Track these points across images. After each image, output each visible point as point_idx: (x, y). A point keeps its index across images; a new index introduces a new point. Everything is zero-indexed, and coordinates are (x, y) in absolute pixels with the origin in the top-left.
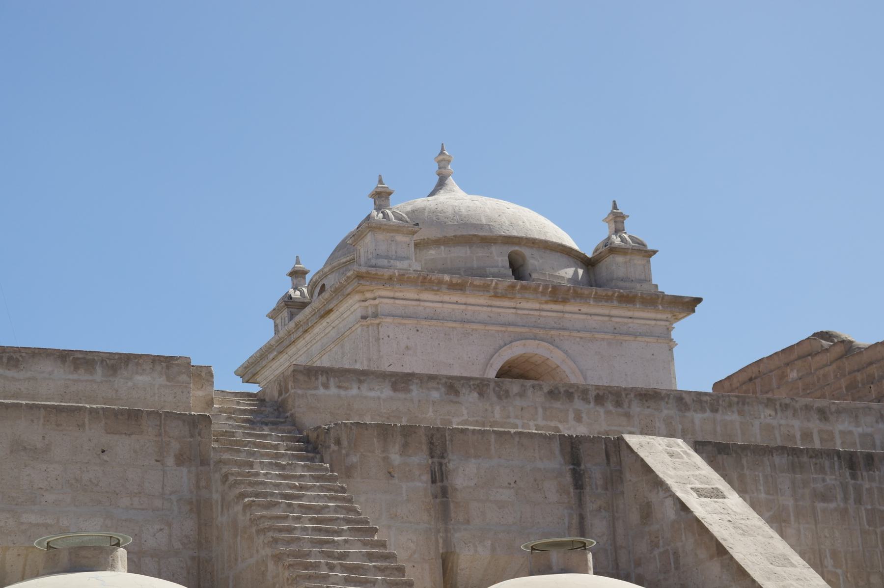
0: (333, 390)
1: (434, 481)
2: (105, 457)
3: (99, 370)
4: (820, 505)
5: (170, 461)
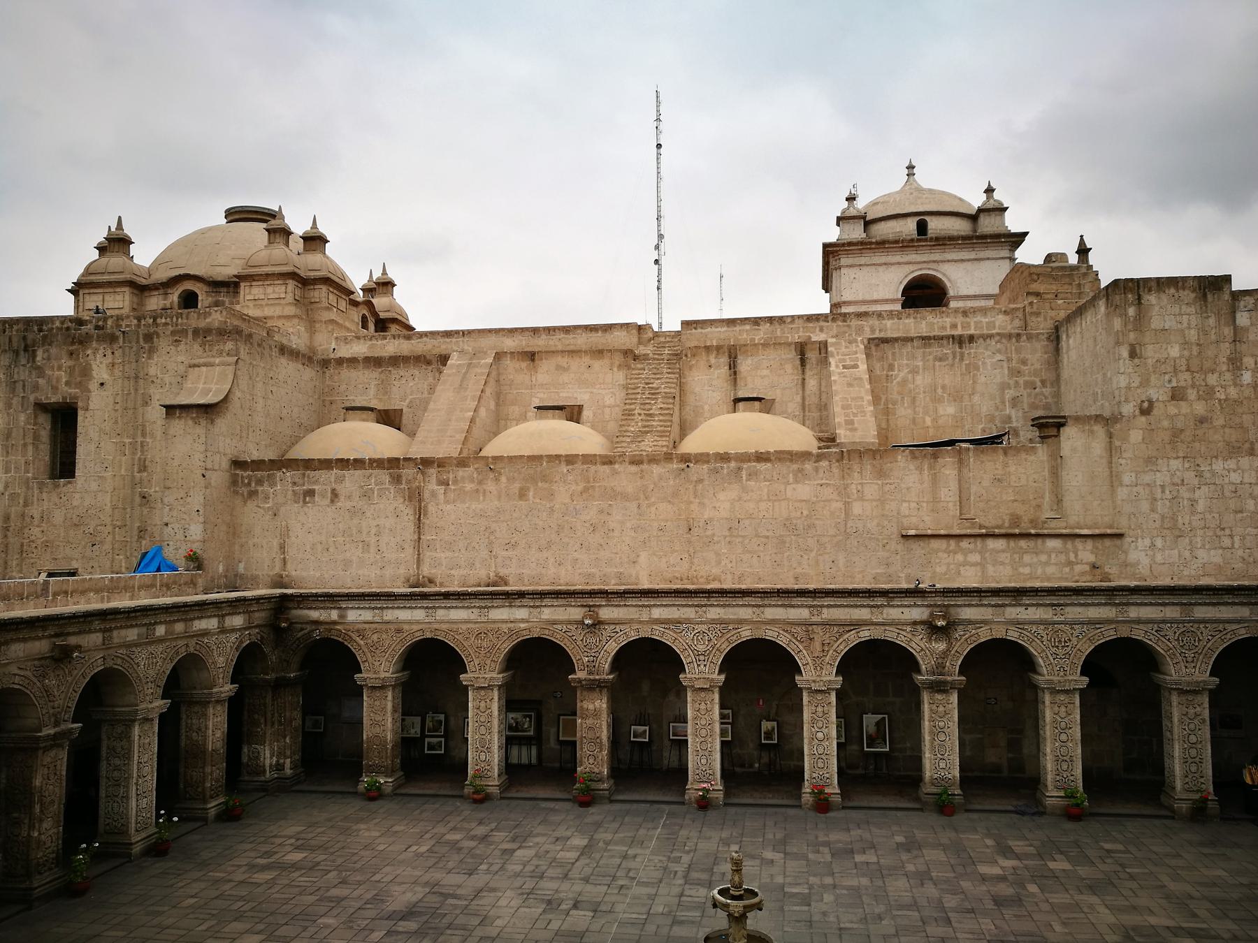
1: (730, 369)
3: (600, 332)
4: (937, 364)
5: (615, 369)
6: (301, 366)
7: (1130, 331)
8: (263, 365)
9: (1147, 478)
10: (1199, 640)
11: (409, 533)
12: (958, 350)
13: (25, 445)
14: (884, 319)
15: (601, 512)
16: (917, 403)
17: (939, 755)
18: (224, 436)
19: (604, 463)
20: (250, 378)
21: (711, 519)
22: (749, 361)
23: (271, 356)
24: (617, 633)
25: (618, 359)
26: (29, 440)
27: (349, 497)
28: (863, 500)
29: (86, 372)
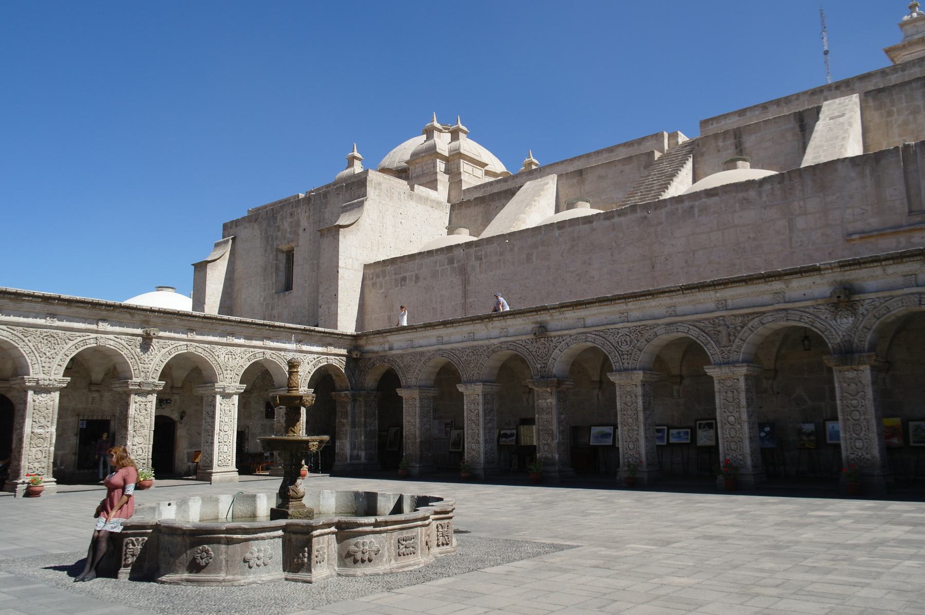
0: (715, 125)
1: (736, 148)
2: (623, 173)
3: (636, 145)
6: (430, 208)
8: (392, 204)
13: (272, 273)
17: (854, 435)
18: (356, 248)
19: (584, 223)
20: (380, 212)
22: (753, 137)
24: (561, 342)
26: (274, 270)
27: (425, 279)
29: (298, 224)
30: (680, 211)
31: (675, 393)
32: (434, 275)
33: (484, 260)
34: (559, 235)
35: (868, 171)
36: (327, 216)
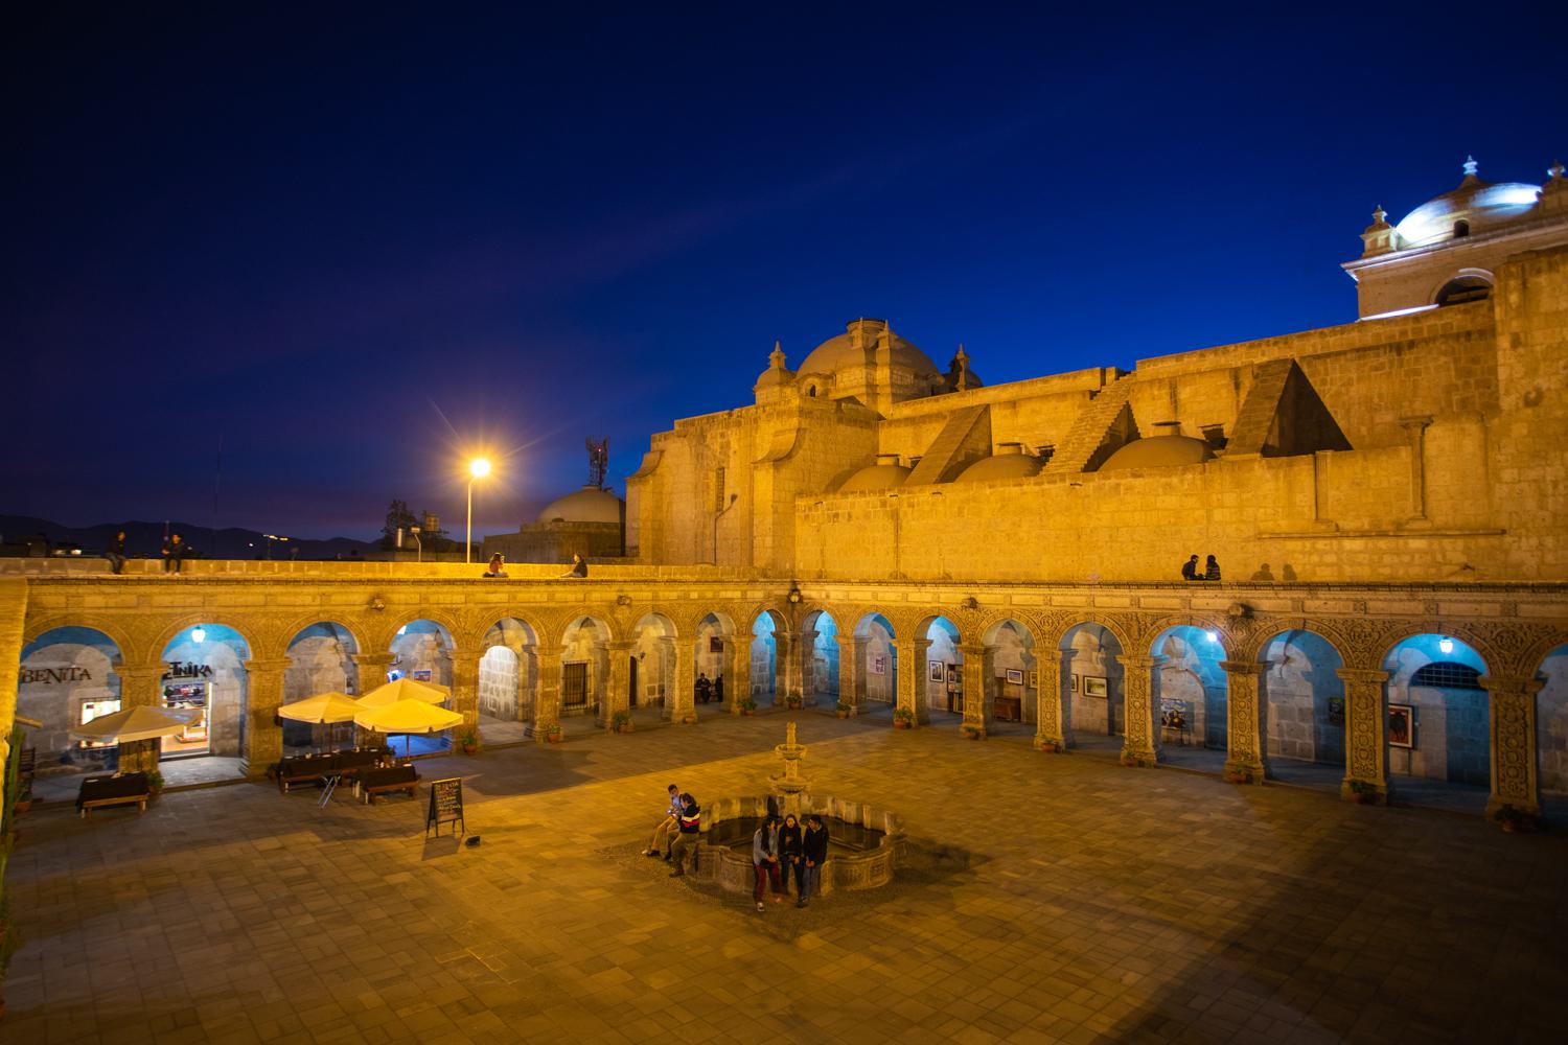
0: (1152, 367)
4: (1373, 373)
6: (859, 429)
7: (1512, 319)
9: (1533, 474)
10: (1522, 641)
11: (891, 544)
12: (1396, 357)
14: (1326, 336)
15: (1014, 524)
16: (1352, 414)
21: (1096, 528)
22: (1188, 389)
23: (830, 425)
25: (1078, 399)
27: (857, 518)
28: (1223, 507)
29: (728, 444)
30: (1107, 487)
31: (1094, 658)
32: (867, 516)
33: (916, 508)
34: (991, 494)
35: (1281, 475)
36: (758, 441)
